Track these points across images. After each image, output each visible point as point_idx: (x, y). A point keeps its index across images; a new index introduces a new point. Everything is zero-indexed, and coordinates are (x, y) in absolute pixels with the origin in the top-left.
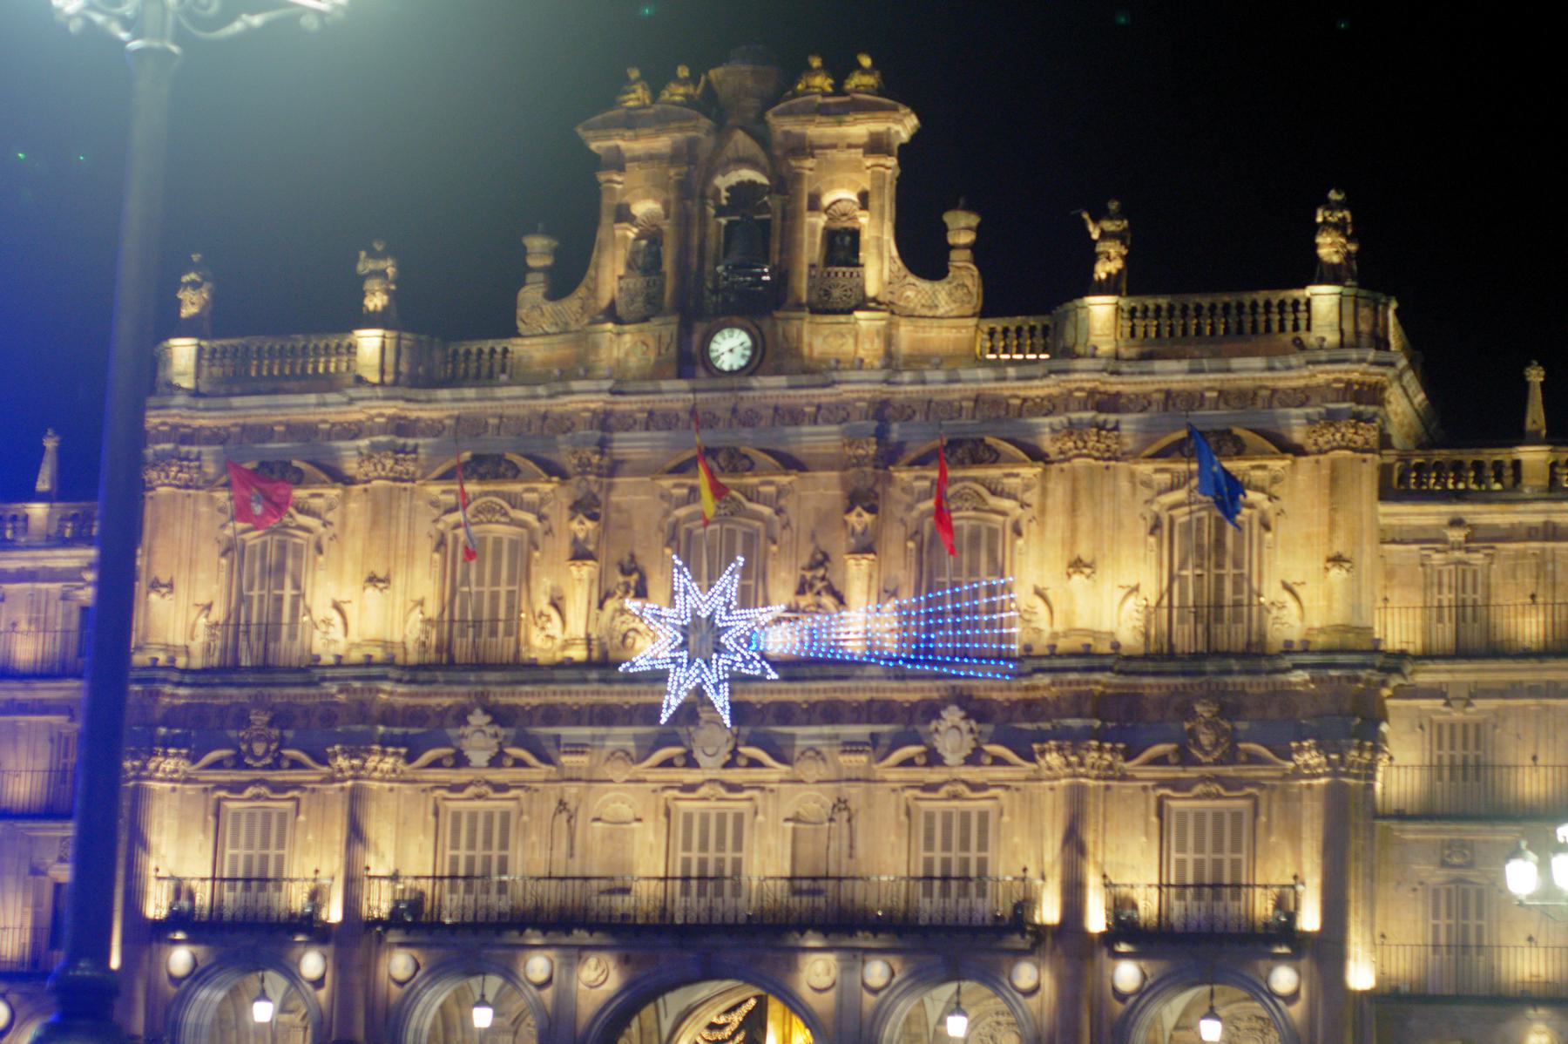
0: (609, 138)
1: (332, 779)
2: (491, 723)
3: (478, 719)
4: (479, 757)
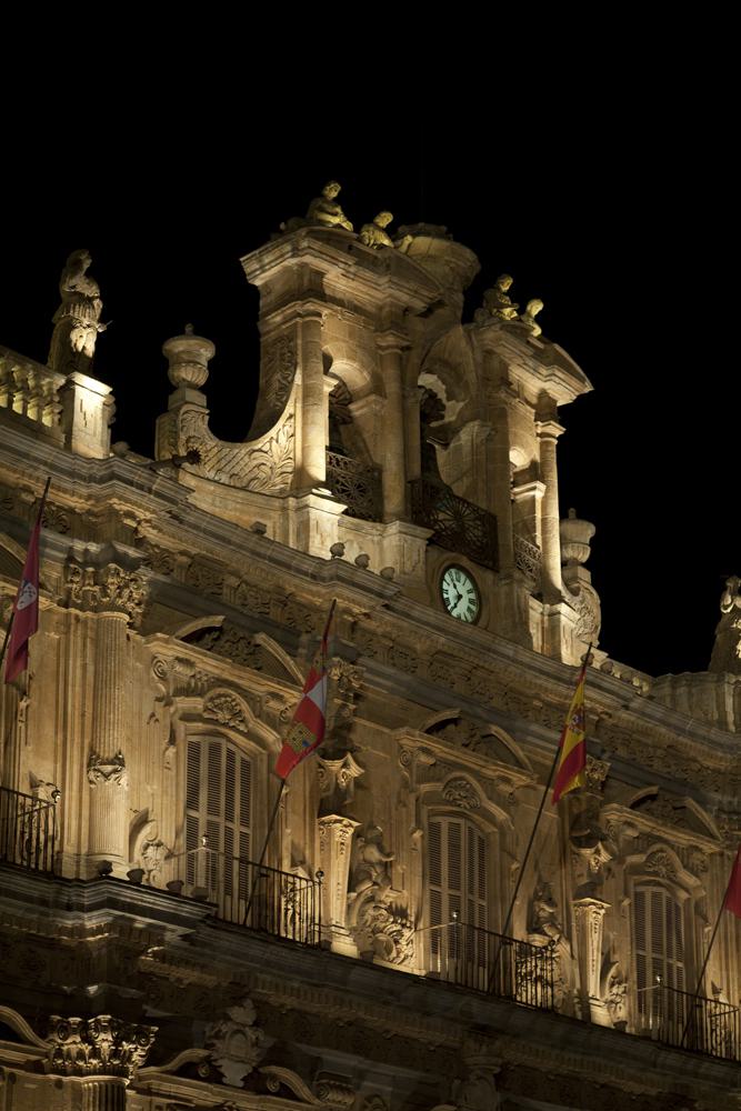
0: (334, 261)
1: (37, 1067)
2: (256, 1024)
3: (242, 1014)
4: (234, 1073)
